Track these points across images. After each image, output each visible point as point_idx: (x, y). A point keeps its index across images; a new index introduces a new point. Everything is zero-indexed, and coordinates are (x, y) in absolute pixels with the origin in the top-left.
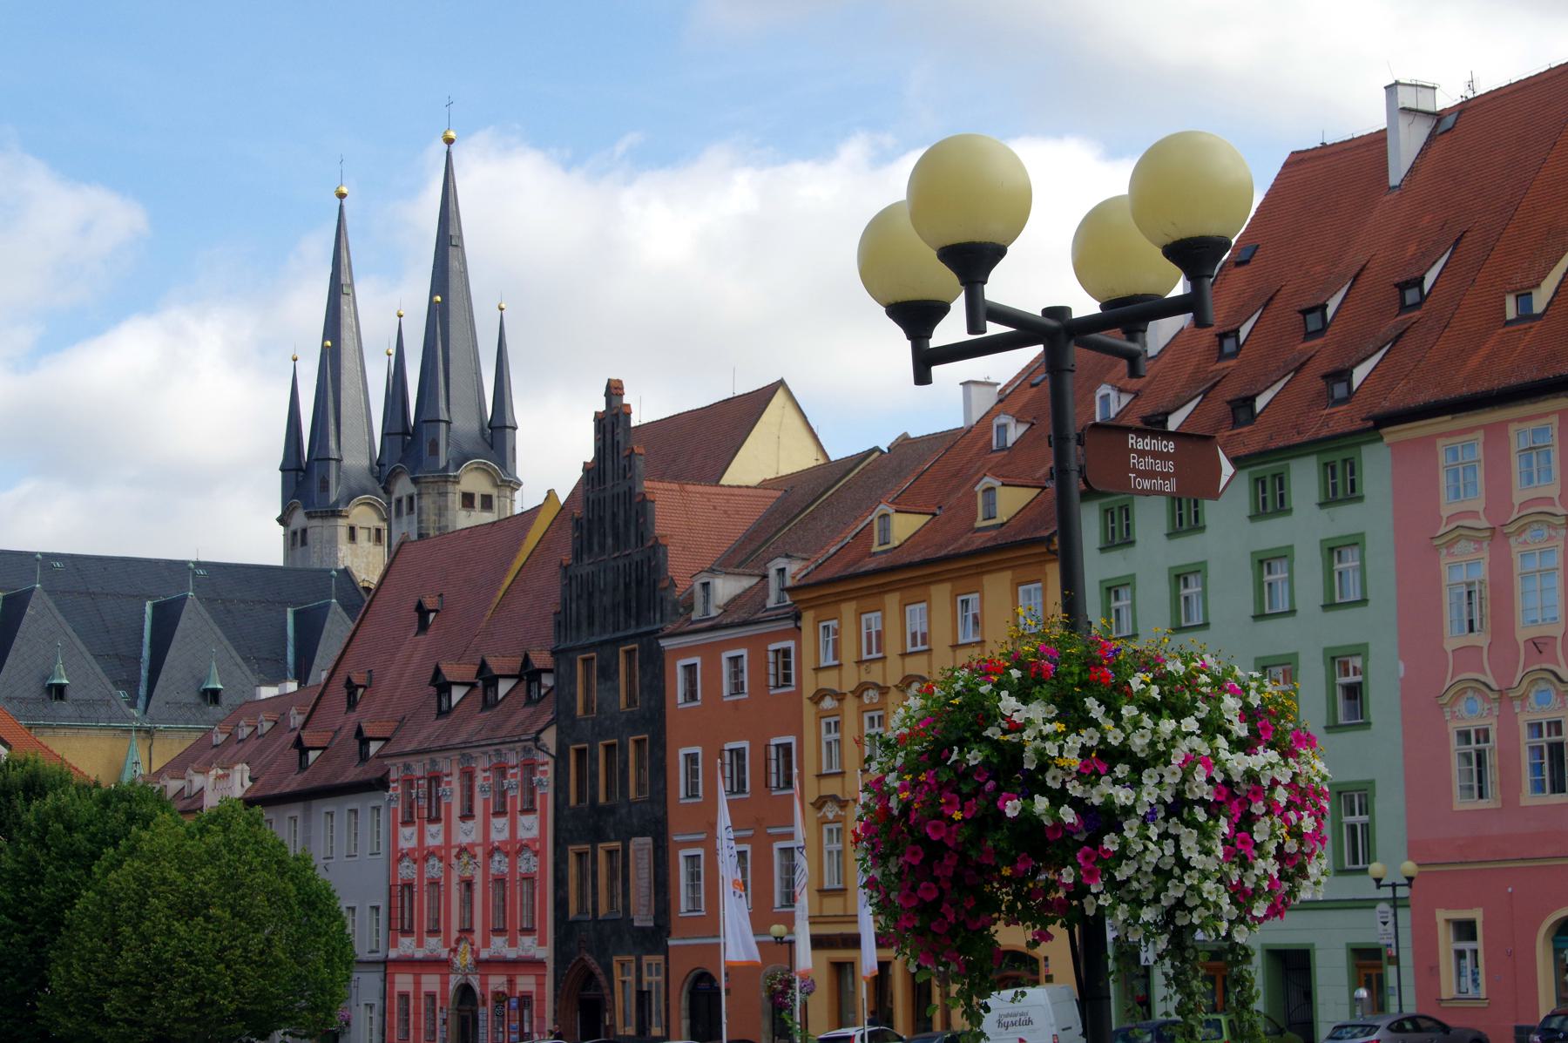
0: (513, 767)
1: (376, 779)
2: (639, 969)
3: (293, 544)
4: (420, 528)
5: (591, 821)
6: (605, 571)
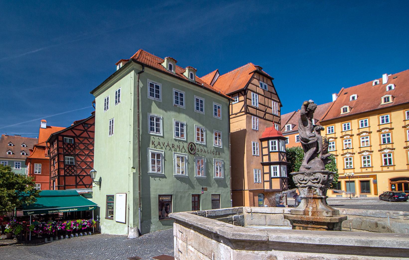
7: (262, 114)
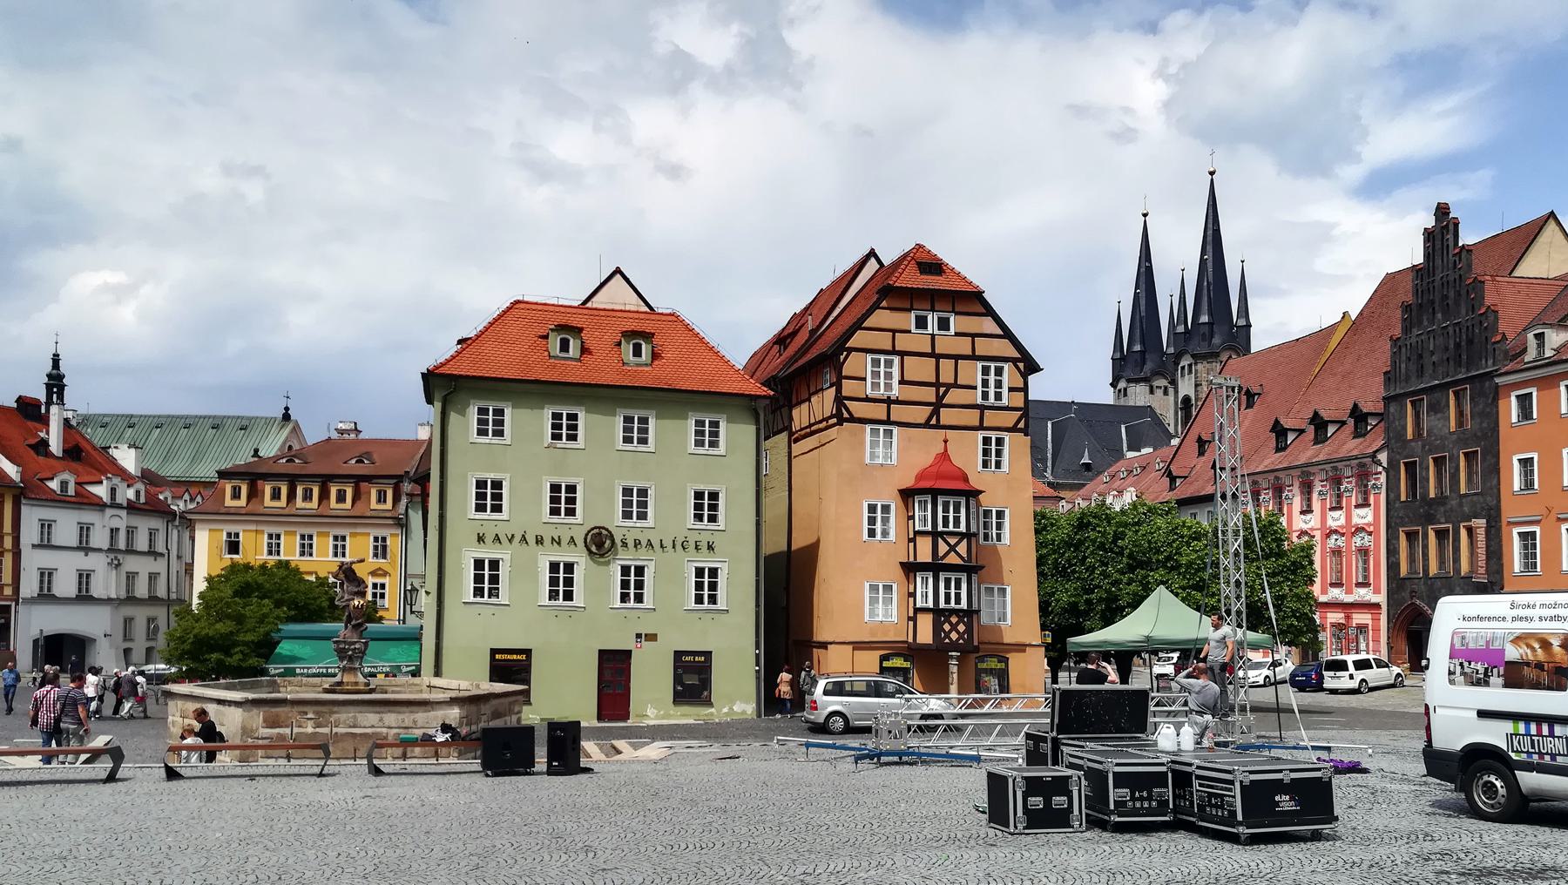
5: (1422, 510)
6: (1434, 337)
7: (921, 414)
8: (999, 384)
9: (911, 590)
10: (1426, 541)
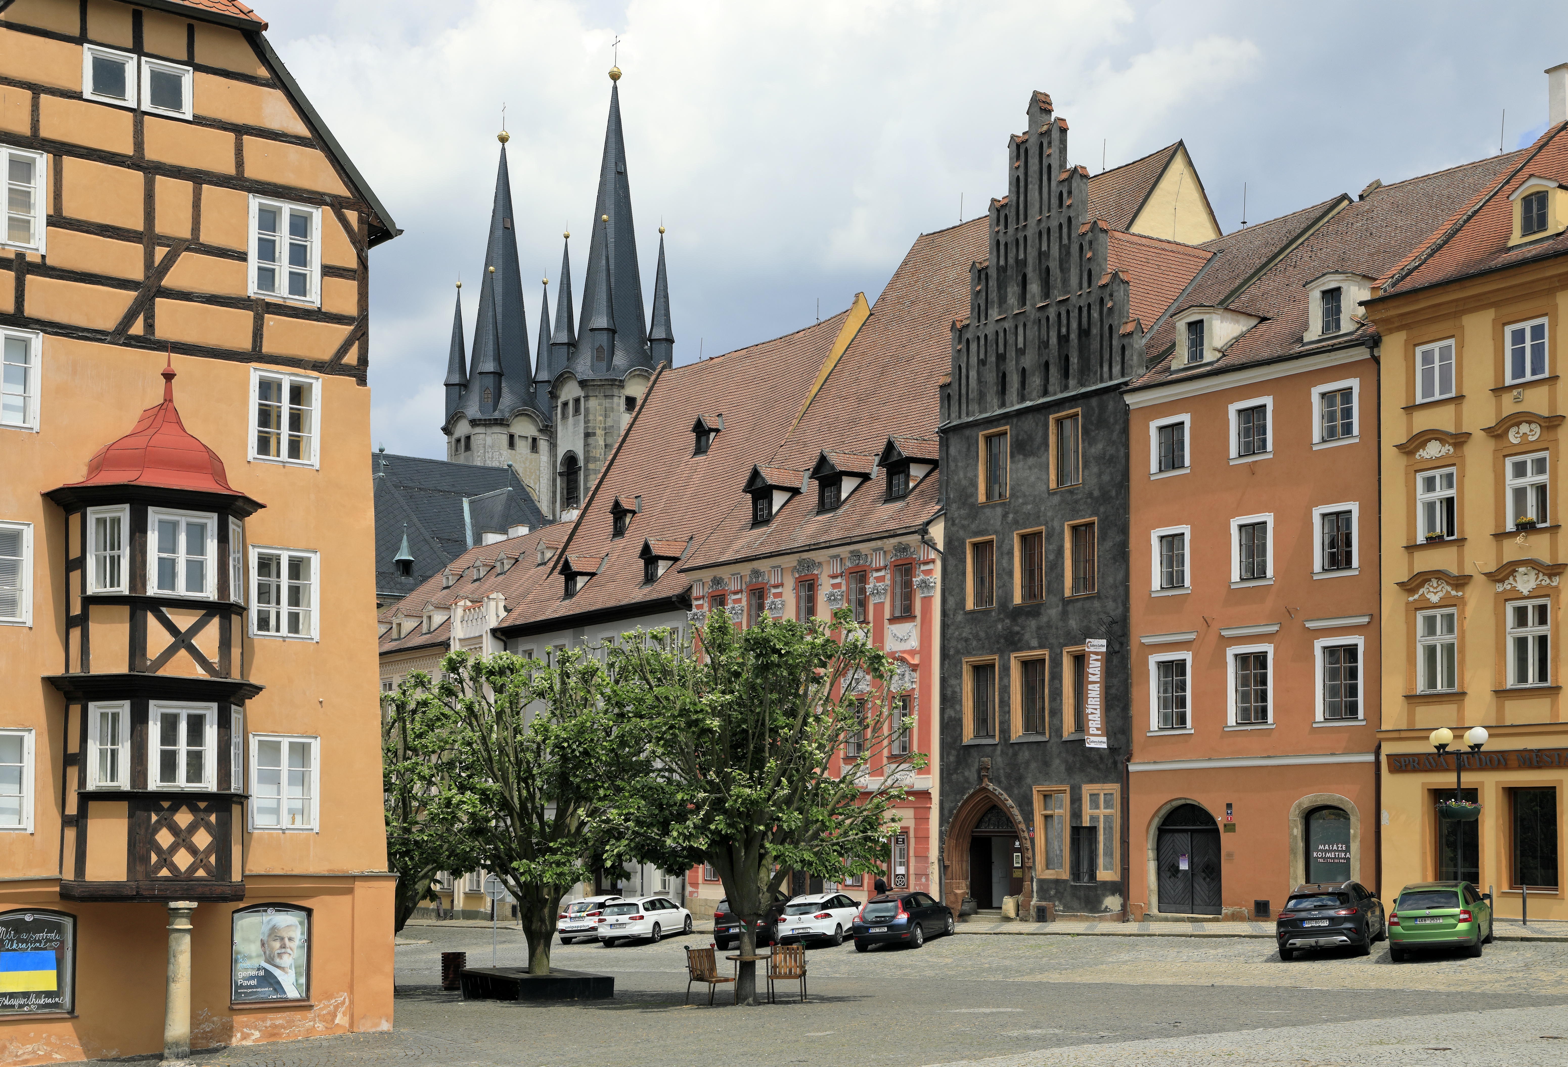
0: (878, 570)
1: (677, 596)
2: (1076, 800)
3: (457, 450)
4: (586, 428)
8: (299, 255)
9: (74, 747)
10: (1005, 681)
